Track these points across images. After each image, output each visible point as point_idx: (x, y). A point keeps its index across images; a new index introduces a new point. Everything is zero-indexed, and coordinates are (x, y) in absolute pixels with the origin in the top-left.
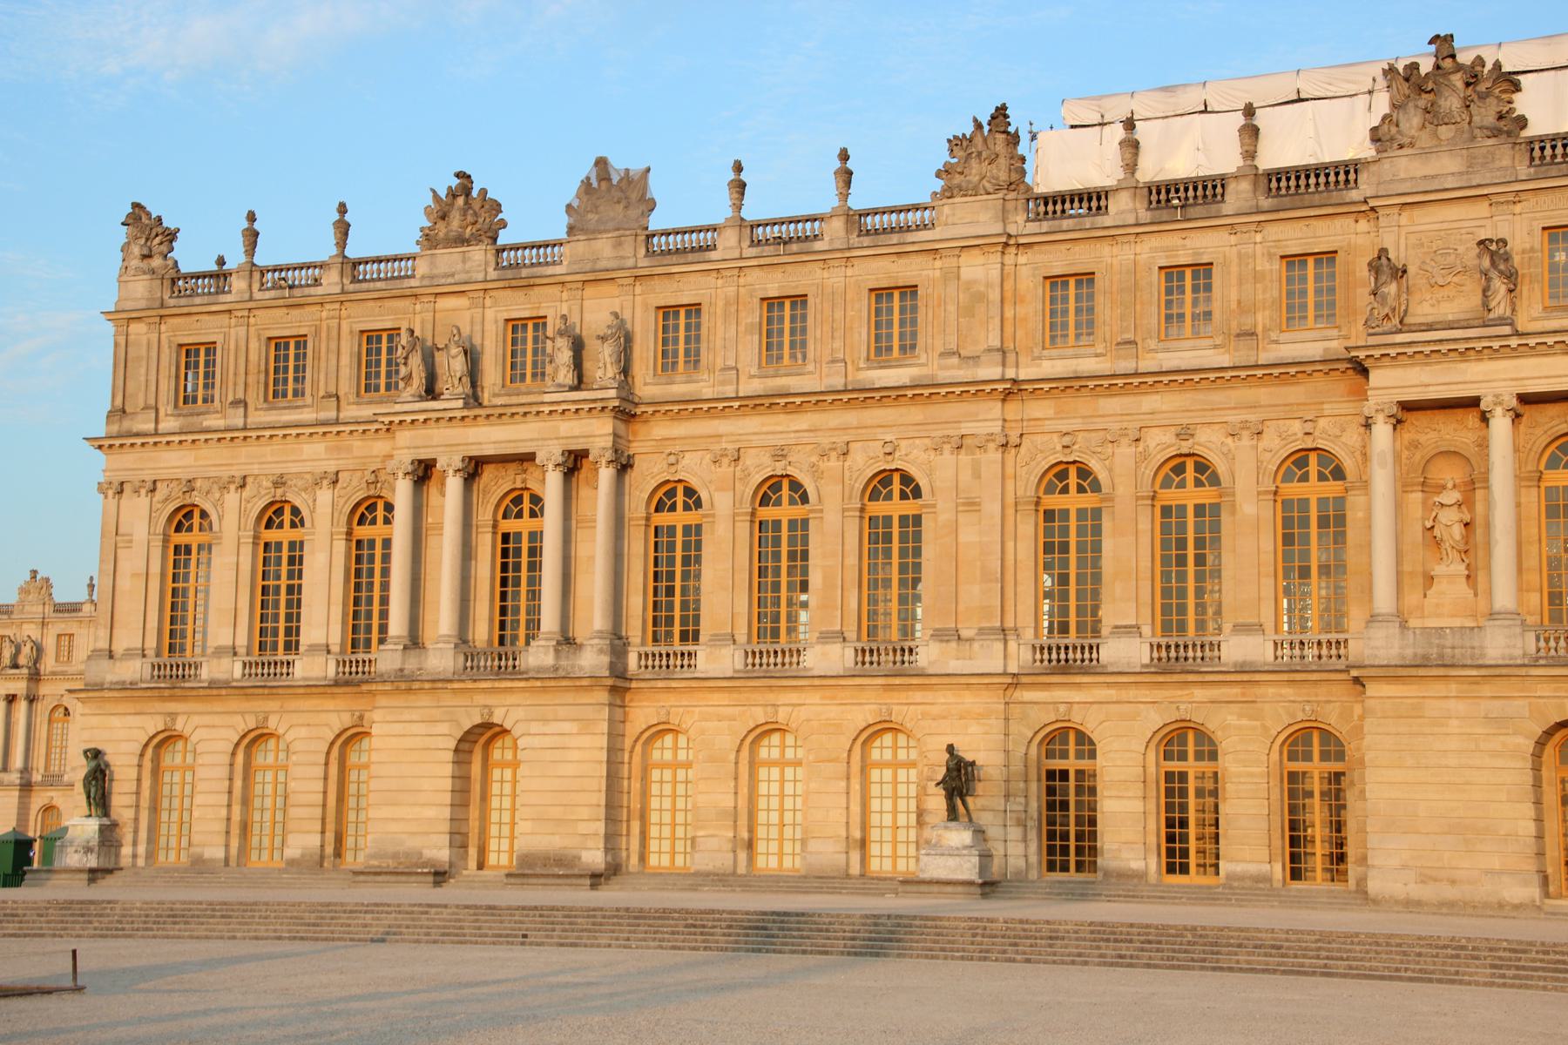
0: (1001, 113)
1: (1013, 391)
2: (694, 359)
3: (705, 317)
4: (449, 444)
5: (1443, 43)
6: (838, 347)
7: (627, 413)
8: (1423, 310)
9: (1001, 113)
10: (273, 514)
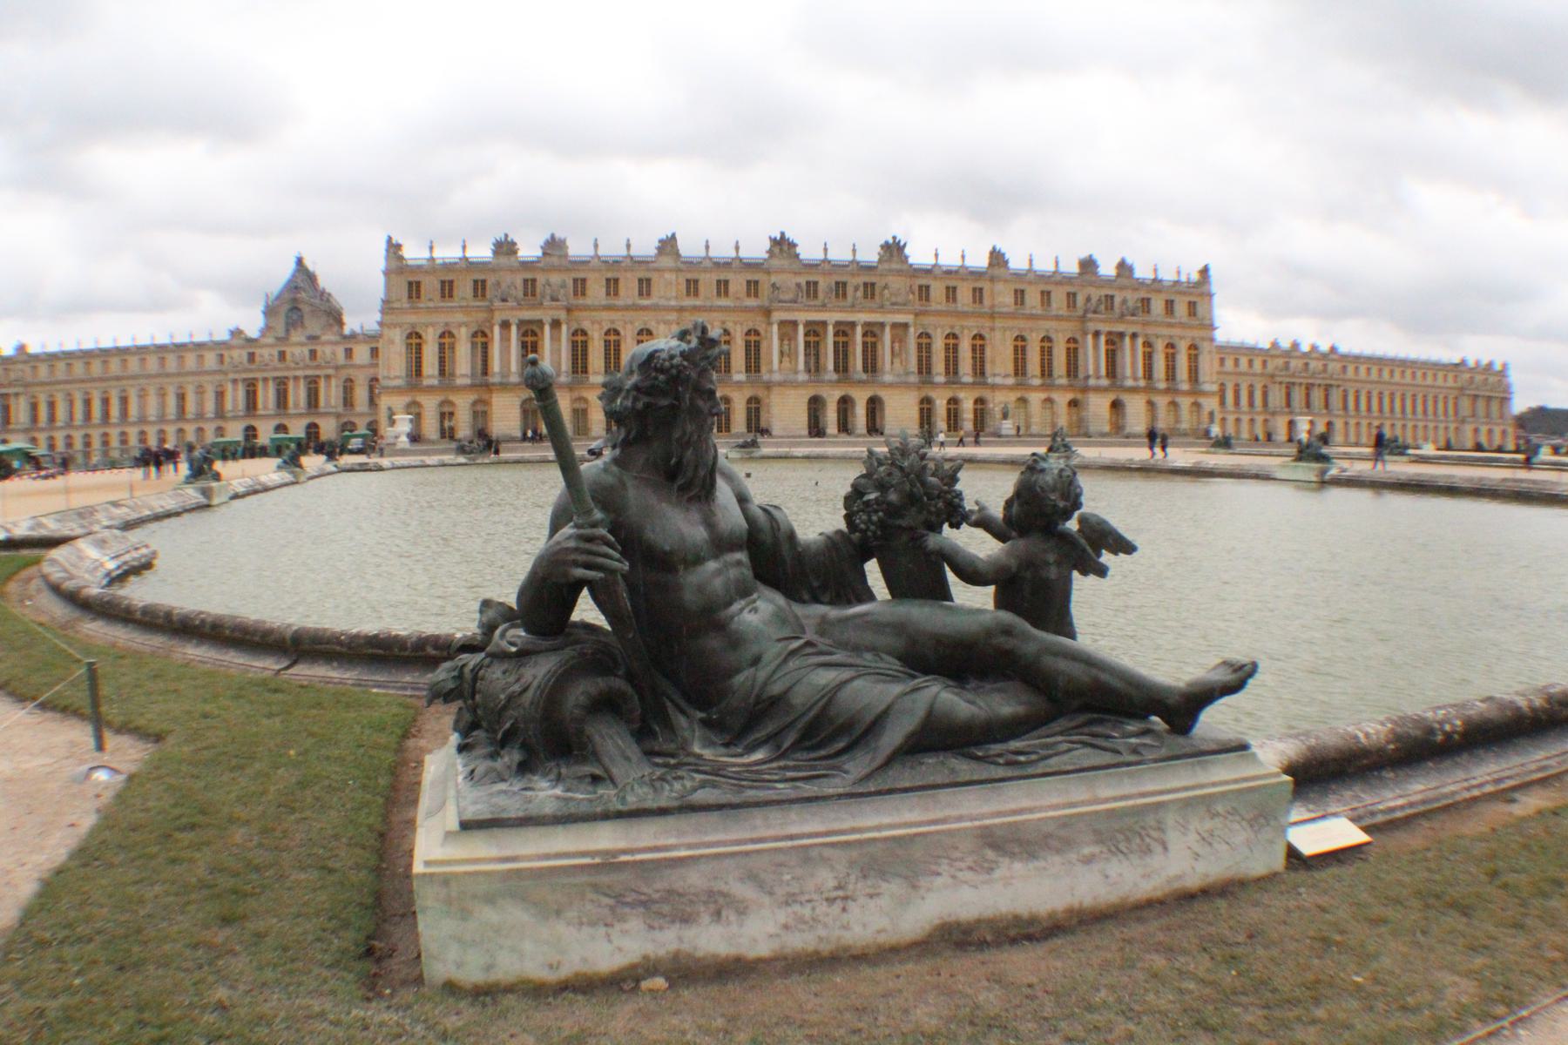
0: (673, 236)
1: (681, 309)
2: (584, 294)
3: (589, 283)
4: (514, 317)
5: (783, 234)
6: (628, 291)
7: (569, 310)
8: (781, 297)
9: (673, 236)
10: (442, 336)
